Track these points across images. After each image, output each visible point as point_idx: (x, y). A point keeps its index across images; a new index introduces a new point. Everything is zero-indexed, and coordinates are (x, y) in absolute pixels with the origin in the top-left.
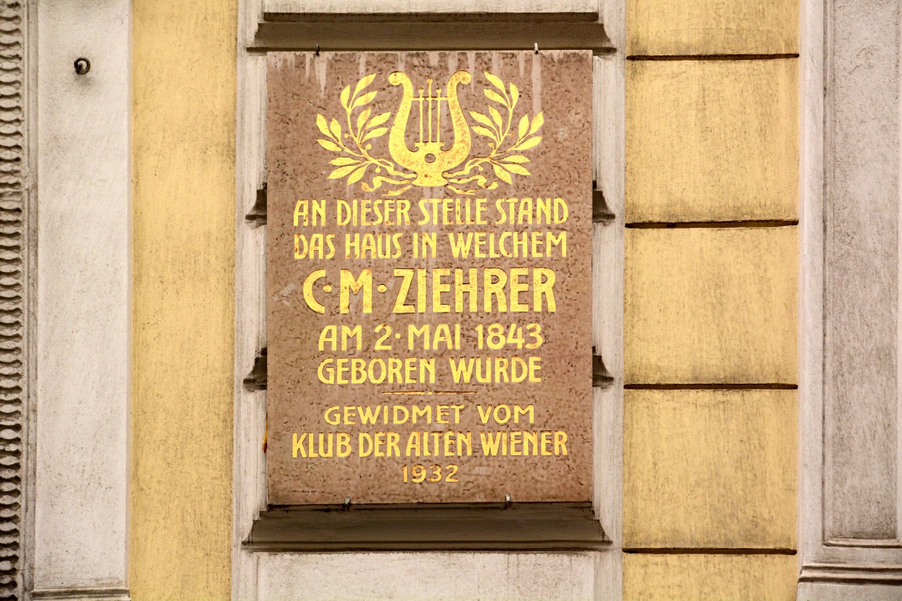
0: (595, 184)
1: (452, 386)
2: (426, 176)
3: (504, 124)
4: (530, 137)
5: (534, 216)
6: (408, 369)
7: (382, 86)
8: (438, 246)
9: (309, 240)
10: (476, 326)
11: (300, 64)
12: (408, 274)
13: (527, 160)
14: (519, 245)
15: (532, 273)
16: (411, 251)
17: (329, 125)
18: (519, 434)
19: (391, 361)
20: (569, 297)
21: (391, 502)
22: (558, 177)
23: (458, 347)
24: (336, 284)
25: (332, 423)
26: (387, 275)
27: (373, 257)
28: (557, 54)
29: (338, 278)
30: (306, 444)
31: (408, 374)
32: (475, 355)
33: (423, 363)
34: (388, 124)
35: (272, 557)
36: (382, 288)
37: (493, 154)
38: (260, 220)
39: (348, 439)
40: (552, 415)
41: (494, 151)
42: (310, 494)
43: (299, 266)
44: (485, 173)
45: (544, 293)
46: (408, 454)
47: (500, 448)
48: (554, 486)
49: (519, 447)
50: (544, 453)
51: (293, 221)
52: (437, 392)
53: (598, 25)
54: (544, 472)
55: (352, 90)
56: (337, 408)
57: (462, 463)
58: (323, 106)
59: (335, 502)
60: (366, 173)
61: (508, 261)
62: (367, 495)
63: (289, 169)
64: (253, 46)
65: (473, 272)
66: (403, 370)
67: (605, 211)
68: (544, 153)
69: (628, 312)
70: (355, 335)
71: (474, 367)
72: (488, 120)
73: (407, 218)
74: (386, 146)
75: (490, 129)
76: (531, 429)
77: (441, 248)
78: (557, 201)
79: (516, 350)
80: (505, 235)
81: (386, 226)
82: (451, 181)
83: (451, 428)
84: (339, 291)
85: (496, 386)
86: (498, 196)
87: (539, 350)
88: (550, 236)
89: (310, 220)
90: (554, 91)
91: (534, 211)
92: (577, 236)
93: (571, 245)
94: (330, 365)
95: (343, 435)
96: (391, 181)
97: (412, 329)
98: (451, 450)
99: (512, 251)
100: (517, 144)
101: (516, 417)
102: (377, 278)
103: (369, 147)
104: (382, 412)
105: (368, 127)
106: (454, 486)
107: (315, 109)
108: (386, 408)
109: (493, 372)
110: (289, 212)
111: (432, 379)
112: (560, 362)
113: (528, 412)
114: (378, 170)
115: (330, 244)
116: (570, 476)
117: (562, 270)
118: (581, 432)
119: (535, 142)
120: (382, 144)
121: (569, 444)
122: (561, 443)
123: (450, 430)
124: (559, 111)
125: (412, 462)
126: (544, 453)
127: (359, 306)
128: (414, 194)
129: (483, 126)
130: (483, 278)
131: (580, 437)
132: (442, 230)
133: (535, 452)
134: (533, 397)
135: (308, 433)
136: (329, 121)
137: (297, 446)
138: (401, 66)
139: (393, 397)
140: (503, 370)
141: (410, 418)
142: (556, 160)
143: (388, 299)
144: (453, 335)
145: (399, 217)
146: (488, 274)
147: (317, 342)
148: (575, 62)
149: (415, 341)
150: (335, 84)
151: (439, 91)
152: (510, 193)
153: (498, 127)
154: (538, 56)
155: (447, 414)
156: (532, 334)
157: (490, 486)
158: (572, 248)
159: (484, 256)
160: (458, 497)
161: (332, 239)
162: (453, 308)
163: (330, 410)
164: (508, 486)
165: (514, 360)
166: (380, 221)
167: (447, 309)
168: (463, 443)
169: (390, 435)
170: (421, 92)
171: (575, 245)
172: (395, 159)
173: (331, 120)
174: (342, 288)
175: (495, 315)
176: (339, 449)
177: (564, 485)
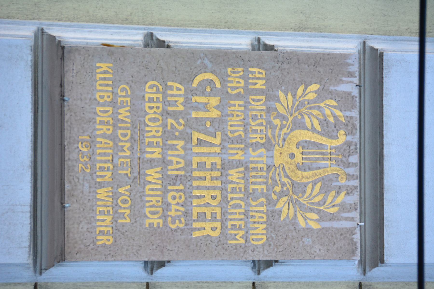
0: (276, 261)
1: (143, 168)
2: (281, 153)
3: (313, 203)
4: (305, 220)
5: (255, 223)
6: (155, 140)
7: (337, 126)
8: (236, 160)
9: (240, 77)
10: (183, 184)
11: (351, 75)
12: (217, 141)
13: (290, 218)
14: (236, 213)
15: (218, 221)
16: (232, 143)
17: (313, 92)
18: (111, 213)
19: (161, 129)
20: (202, 245)
21: (65, 127)
22: (280, 238)
23: (169, 173)
24: (211, 94)
25: (119, 90)
26: (217, 127)
27: (229, 119)
28: (357, 238)
29: (215, 96)
30: (105, 72)
31: (151, 140)
32: (164, 184)
33: (159, 150)
34: (314, 130)
35: (30, 48)
36: (208, 124)
37: (295, 197)
38: (257, 47)
39: (108, 100)
40: (123, 234)
41: (296, 197)
42: (71, 74)
43: (223, 71)
44: (283, 191)
45: (204, 229)
46: (98, 139)
47: (102, 200)
48: (76, 236)
49: (102, 213)
50: (98, 229)
51: (252, 67)
52: (139, 158)
53: (378, 263)
54: (85, 229)
55: (335, 107)
56: (129, 93)
57: (92, 175)
58: (325, 88)
59: (66, 90)
60: (282, 115)
61: (225, 206)
62: (71, 112)
63: (285, 66)
64: (366, 45)
65: (218, 183)
66: (154, 137)
67: (262, 268)
68: (295, 229)
69: (197, 284)
70: (177, 106)
71: (156, 184)
72: (316, 193)
73: (254, 141)
74: (300, 128)
75: (311, 194)
76: (115, 220)
77: (235, 163)
78: (264, 237)
79: (167, 210)
80: (242, 203)
81: (248, 127)
82: (278, 169)
83: (115, 168)
84: (206, 96)
85: (143, 198)
86: (267, 199)
87: (167, 226)
88: (241, 233)
89: (253, 79)
90: (334, 235)
91: (258, 223)
92: (242, 250)
93: (236, 247)
94: (158, 89)
95: (111, 97)
96: (277, 130)
97: (181, 143)
98: (100, 168)
99: (233, 208)
100: (300, 212)
101: (123, 211)
102: (215, 120)
103: (299, 117)
104: (126, 122)
105: (311, 116)
106: (76, 169)
107: (323, 83)
108: (129, 125)
109: (152, 196)
110: (258, 65)
111: (148, 156)
112: (159, 239)
113: (126, 219)
114: (284, 122)
115: (238, 91)
116: (82, 246)
117: (220, 241)
118: (112, 253)
119: (302, 223)
120: (301, 125)
121: (104, 246)
122: (105, 240)
123: (114, 167)
124: (321, 238)
125: (93, 142)
126: (98, 229)
127: (197, 109)
128: (268, 145)
129: (313, 189)
130: (214, 189)
131: (108, 253)
132: (246, 163)
133: (99, 223)
134: (136, 222)
135: (112, 74)
136: (316, 92)
137: (104, 66)
138: (349, 138)
139: (136, 130)
140: (154, 202)
141: (122, 141)
142: (290, 236)
143: (201, 128)
144: (178, 170)
145: (254, 136)
146: (217, 193)
147: (173, 81)
148: (352, 249)
149: (174, 145)
150: (338, 96)
151: (334, 162)
152: (270, 207)
153: (311, 200)
154: (356, 225)
155: (125, 166)
156: (177, 221)
157: (75, 193)
158: (234, 247)
159: (229, 190)
160: (69, 172)
161: (240, 92)
162: (195, 170)
163: (128, 89)
164: (75, 205)
165: (160, 209)
166: (252, 123)
167: (195, 166)
168: (105, 176)
169: (111, 127)
170: (333, 151)
171: (236, 249)
172: (292, 134)
173: (316, 93)
174: (208, 98)
175: (190, 197)
176: (102, 94)
177: (76, 243)
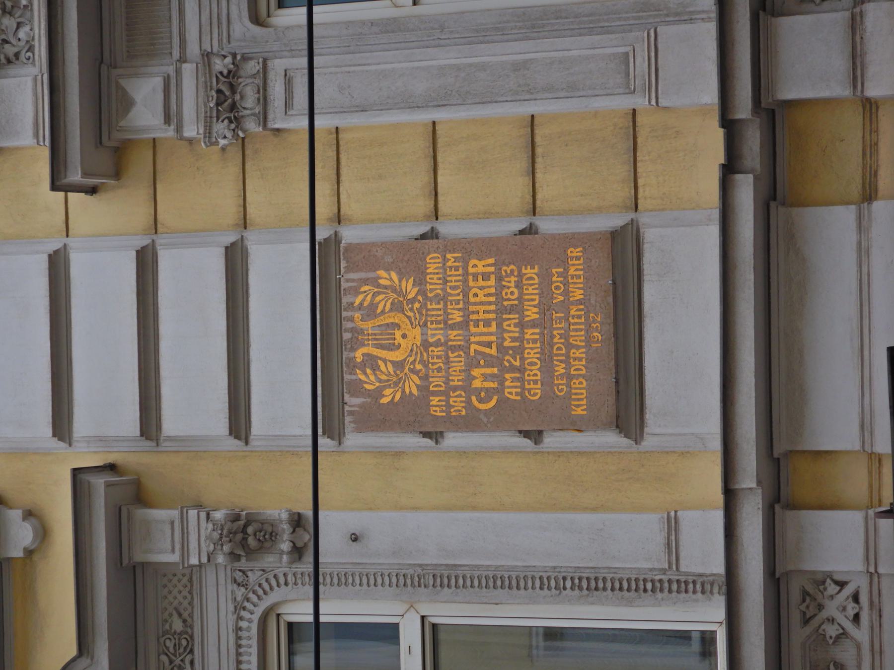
0: (416, 239)
6: (531, 345)
7: (363, 366)
9: (454, 406)
11: (351, 413)
12: (473, 347)
16: (459, 346)
19: (526, 356)
23: (517, 316)
28: (343, 264)
30: (578, 406)
31: (534, 346)
33: (527, 336)
34: (385, 361)
37: (401, 299)
39: (575, 381)
44: (413, 303)
46: (583, 344)
47: (579, 288)
49: (578, 277)
50: (581, 261)
54: (593, 261)
55: (366, 383)
57: (588, 311)
65: (471, 308)
66: (532, 349)
73: (440, 349)
74: (397, 362)
76: (566, 270)
78: (428, 261)
86: (426, 295)
87: (518, 267)
88: (449, 264)
97: (506, 344)
103: (398, 372)
104: (558, 361)
109: (532, 294)
111: (537, 331)
114: (412, 367)
115: (456, 394)
119: (394, 275)
121: (575, 247)
127: (493, 377)
128: (426, 345)
136: (384, 396)
137: (579, 411)
138: (352, 355)
140: (530, 288)
143: (489, 359)
144: (510, 319)
146: (472, 299)
162: (493, 320)
165: (525, 282)
166: (441, 365)
167: (494, 323)
169: (572, 355)
